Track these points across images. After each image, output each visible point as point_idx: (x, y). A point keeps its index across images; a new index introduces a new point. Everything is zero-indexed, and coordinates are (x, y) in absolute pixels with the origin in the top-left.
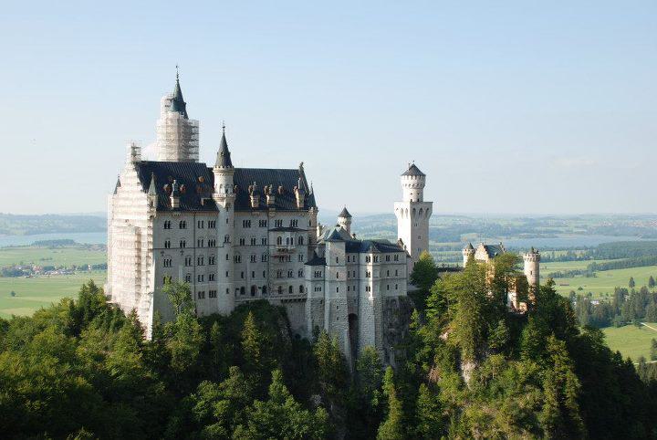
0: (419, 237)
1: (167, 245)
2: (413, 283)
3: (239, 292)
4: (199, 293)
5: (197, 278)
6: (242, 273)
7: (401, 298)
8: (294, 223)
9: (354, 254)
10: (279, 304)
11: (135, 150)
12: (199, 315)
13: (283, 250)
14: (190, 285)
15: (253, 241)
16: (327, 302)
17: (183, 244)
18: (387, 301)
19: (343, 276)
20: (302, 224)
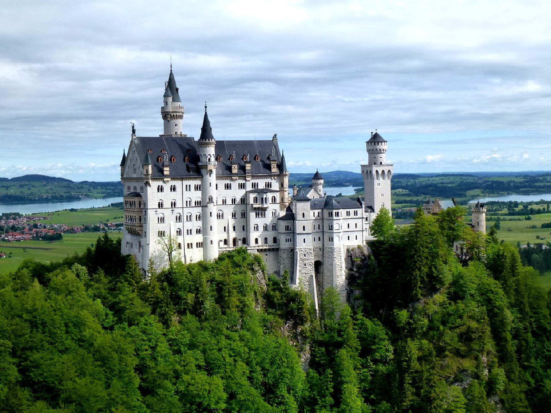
0: (383, 195)
1: (160, 205)
2: (373, 234)
3: (222, 244)
4: (188, 244)
5: (185, 232)
6: (225, 227)
7: (359, 247)
8: (269, 185)
9: (320, 211)
10: (256, 253)
11: (134, 131)
12: (188, 262)
13: (259, 208)
14: (180, 239)
15: (234, 201)
16: (297, 250)
17: (174, 204)
18: (348, 250)
19: (309, 229)
20: (275, 186)
